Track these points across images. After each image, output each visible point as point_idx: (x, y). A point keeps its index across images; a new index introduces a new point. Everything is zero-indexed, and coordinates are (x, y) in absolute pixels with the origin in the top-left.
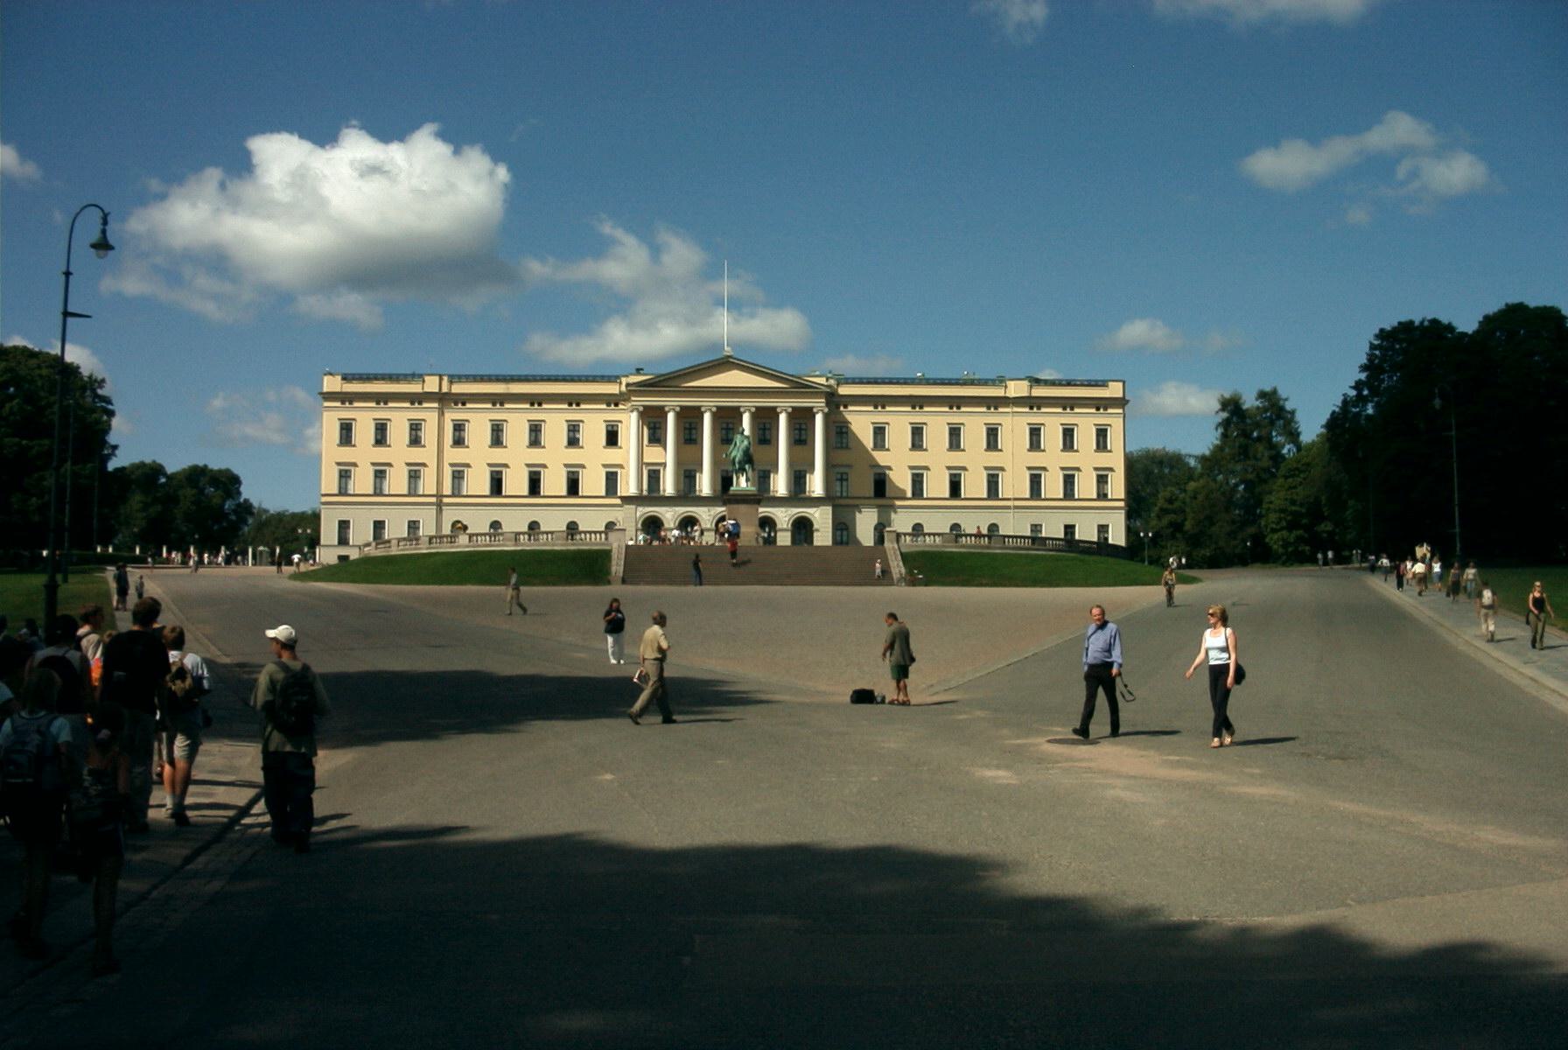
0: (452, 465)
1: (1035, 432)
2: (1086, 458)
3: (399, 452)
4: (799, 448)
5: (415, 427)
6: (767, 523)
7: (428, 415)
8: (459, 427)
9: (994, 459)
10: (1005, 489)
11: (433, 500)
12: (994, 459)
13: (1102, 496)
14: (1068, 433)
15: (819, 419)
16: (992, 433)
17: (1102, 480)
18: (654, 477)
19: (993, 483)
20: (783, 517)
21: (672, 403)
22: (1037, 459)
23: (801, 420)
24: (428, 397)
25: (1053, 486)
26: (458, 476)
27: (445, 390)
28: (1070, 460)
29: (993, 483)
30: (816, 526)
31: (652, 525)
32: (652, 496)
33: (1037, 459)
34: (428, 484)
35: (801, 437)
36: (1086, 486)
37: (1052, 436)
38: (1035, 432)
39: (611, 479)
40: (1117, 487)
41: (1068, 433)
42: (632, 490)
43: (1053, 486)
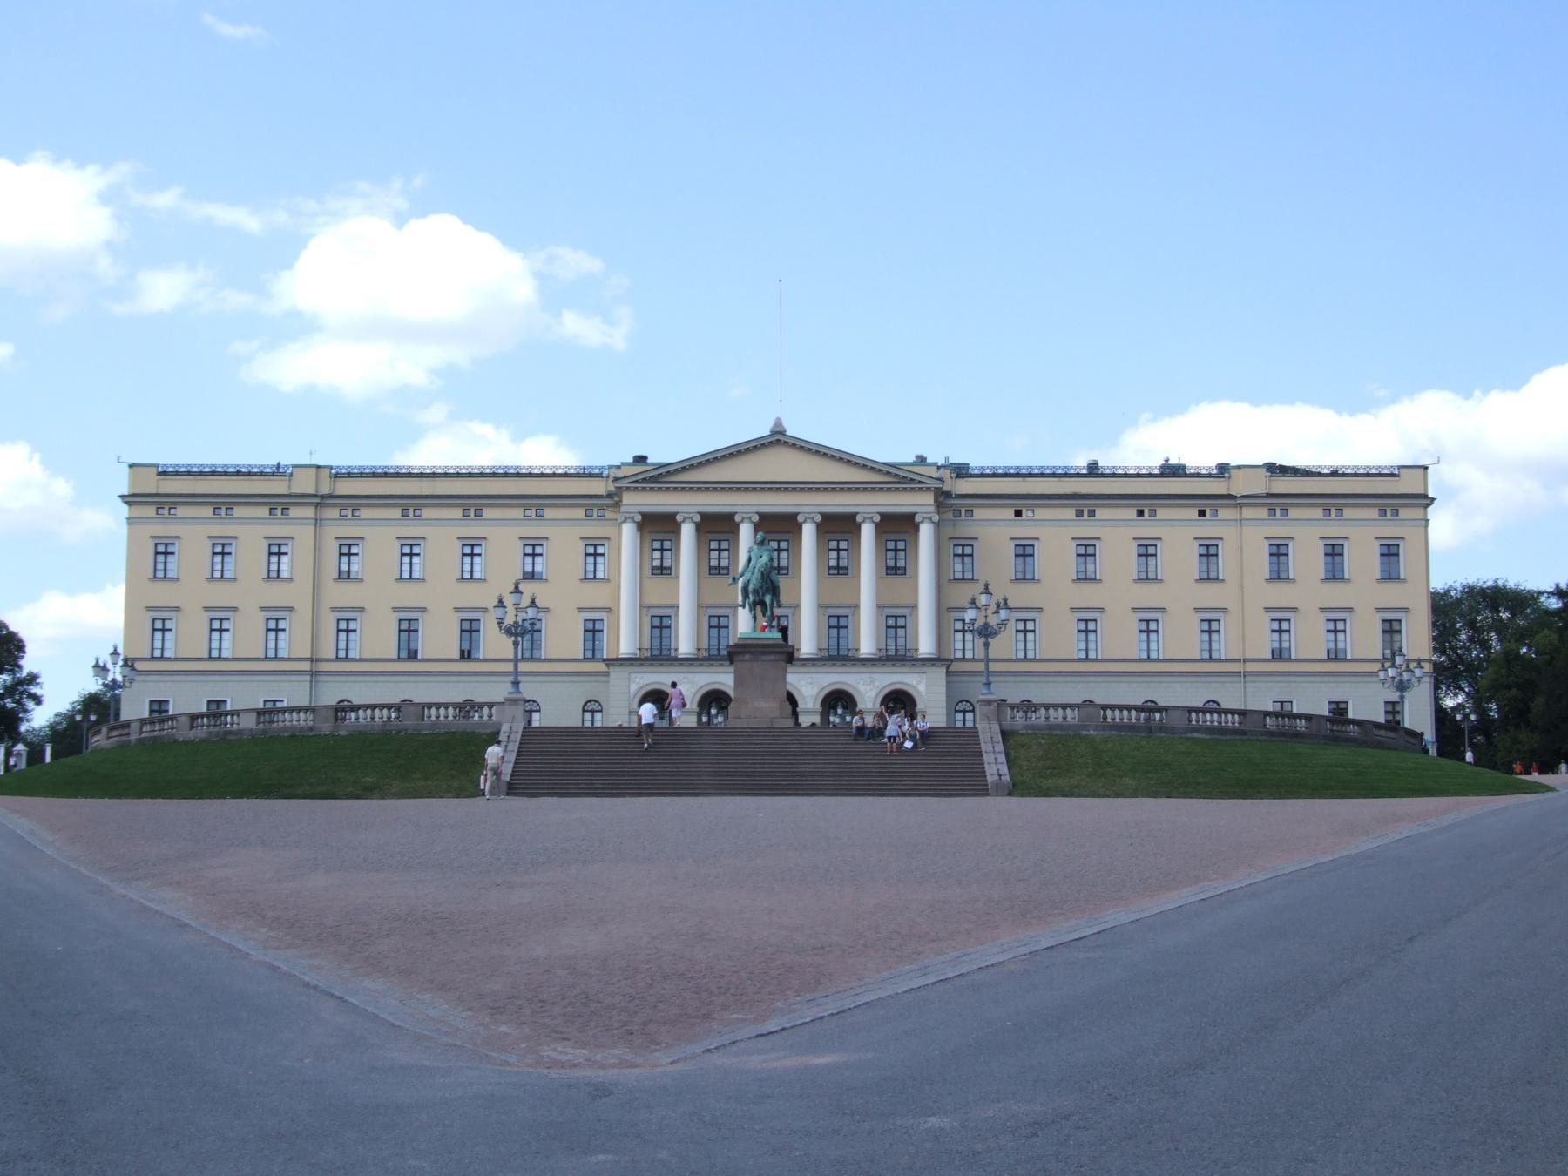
0: (334, 609)
1: (1279, 551)
2: (1364, 590)
3: (249, 591)
4: (896, 581)
5: (276, 549)
6: (839, 700)
7: (299, 528)
8: (347, 549)
9: (1210, 595)
10: (1227, 645)
11: (306, 666)
12: (1210, 595)
13: (1393, 652)
14: (1334, 552)
15: (926, 532)
16: (1209, 552)
17: (1391, 629)
18: (661, 624)
20: (868, 689)
21: (687, 505)
22: (1280, 595)
23: (897, 528)
24: (300, 499)
26: (345, 629)
27: (326, 490)
28: (1336, 595)
30: (920, 706)
32: (659, 655)
33: (1280, 595)
34: (295, 642)
35: (895, 568)
36: (1365, 640)
37: (1307, 558)
38: (1279, 551)
39: (592, 631)
40: (1418, 640)
41: (1334, 552)
42: (626, 648)
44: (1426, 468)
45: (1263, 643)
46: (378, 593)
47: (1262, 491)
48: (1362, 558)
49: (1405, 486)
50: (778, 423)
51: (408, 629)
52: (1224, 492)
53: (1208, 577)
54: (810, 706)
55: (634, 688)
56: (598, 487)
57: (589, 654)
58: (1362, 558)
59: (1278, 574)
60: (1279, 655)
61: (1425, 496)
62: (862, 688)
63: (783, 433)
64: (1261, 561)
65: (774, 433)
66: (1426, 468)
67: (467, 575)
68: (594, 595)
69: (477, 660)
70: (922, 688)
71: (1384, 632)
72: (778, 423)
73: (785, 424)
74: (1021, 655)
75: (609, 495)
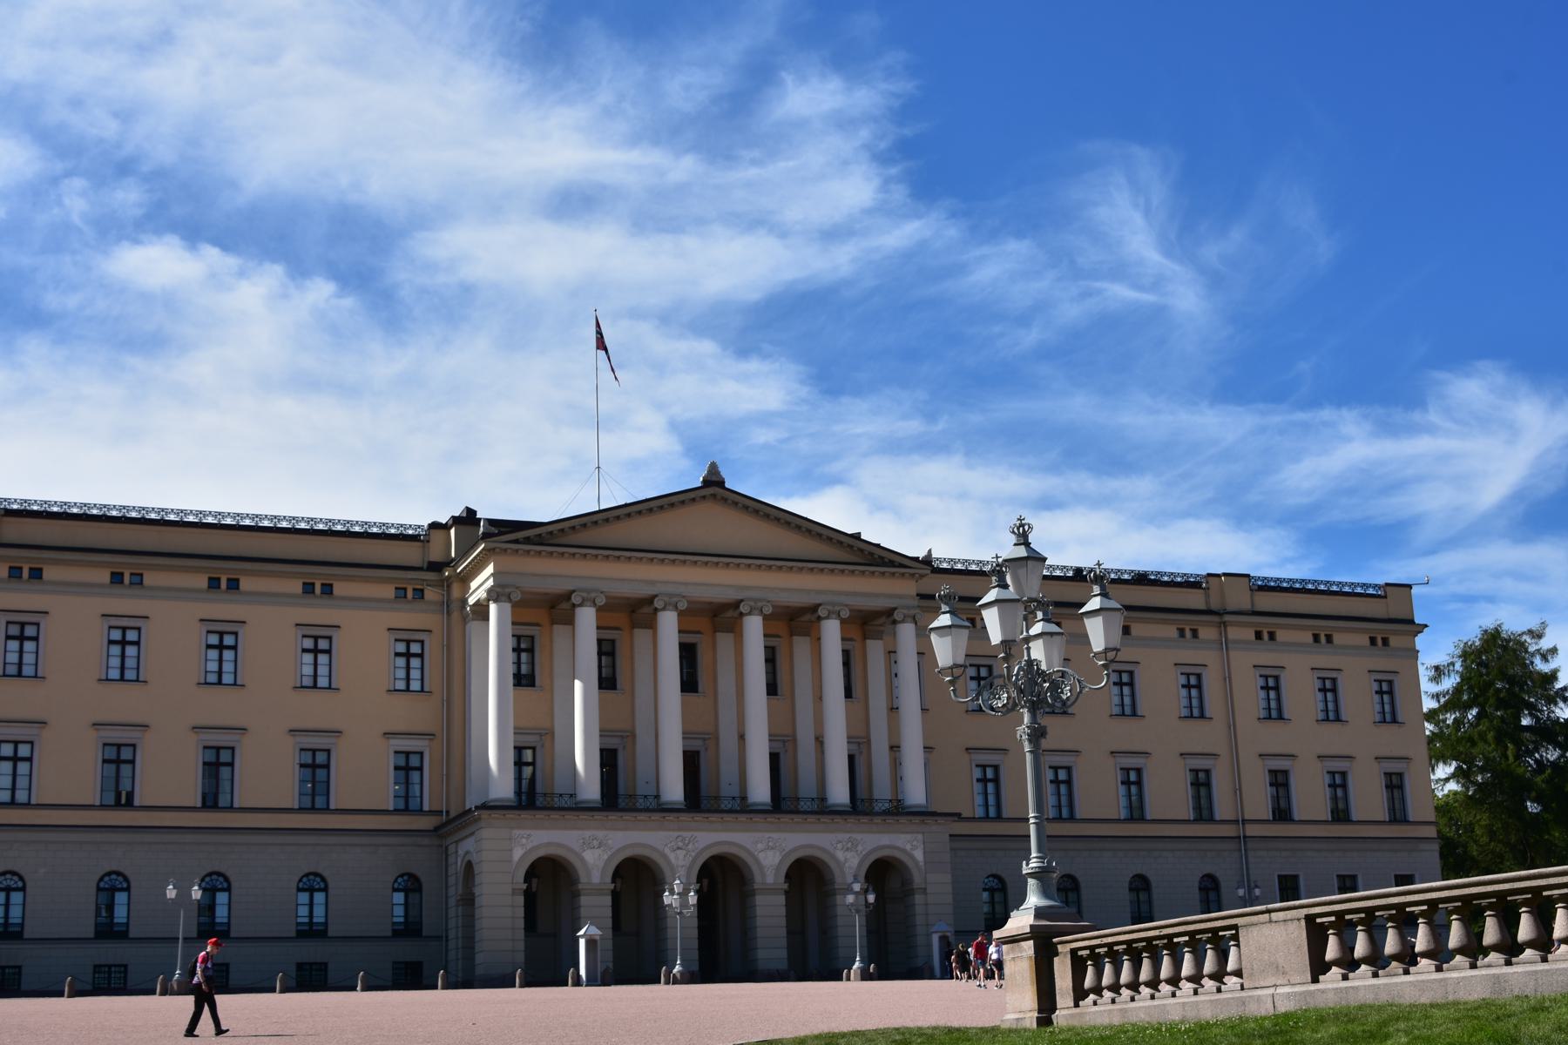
1: (1272, 685)
6: (807, 877)
14: (1329, 687)
16: (1193, 683)
19: (1201, 782)
22: (1275, 738)
25: (1310, 798)
28: (1333, 739)
29: (1201, 782)
30: (917, 880)
31: (549, 881)
33: (1275, 738)
37: (1301, 694)
38: (1272, 685)
39: (407, 767)
41: (1329, 687)
43: (1310, 798)
44: (1410, 586)
45: (1259, 802)
46: (68, 697)
47: (1247, 606)
48: (1358, 697)
49: (1392, 609)
50: (713, 468)
51: (119, 758)
52: (1202, 606)
53: (1197, 713)
54: (770, 879)
55: (518, 854)
56: (410, 554)
57: (402, 806)
58: (1358, 697)
59: (1275, 713)
60: (1282, 814)
61: (1412, 622)
62: (840, 855)
63: (721, 484)
64: (1250, 697)
65: (707, 483)
66: (1410, 586)
67: (212, 678)
68: (413, 714)
69: (231, 808)
70: (919, 855)
71: (1387, 787)
72: (713, 468)
73: (725, 473)
74: (980, 812)
75: (436, 567)
